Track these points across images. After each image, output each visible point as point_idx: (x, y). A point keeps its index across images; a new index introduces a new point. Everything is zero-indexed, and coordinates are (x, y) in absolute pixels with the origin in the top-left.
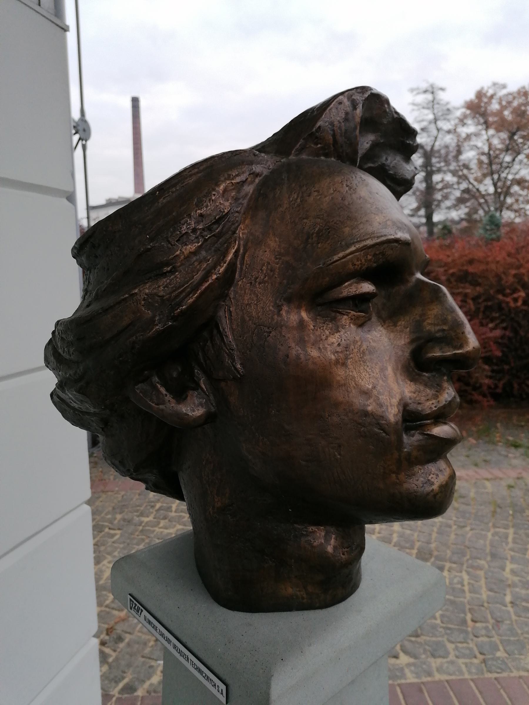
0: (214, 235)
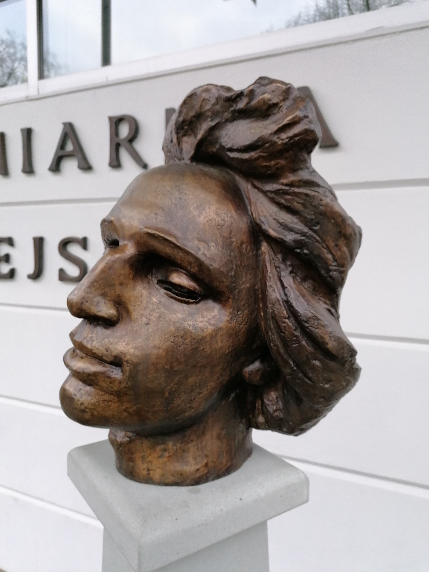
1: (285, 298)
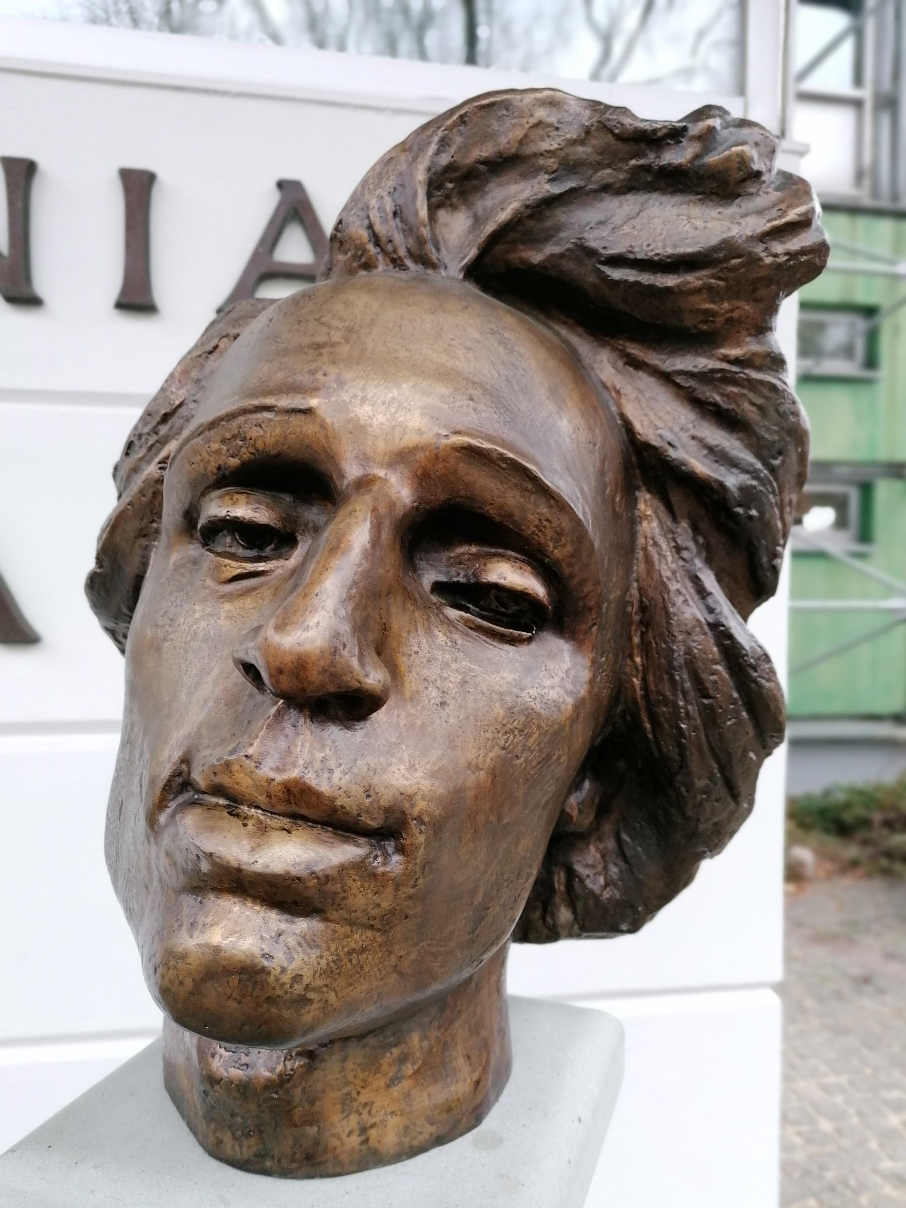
0: (157, 441)
1: (710, 619)
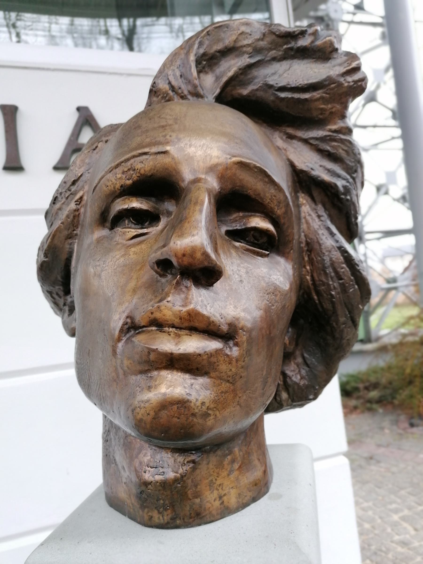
0: (71, 194)
1: (338, 245)
